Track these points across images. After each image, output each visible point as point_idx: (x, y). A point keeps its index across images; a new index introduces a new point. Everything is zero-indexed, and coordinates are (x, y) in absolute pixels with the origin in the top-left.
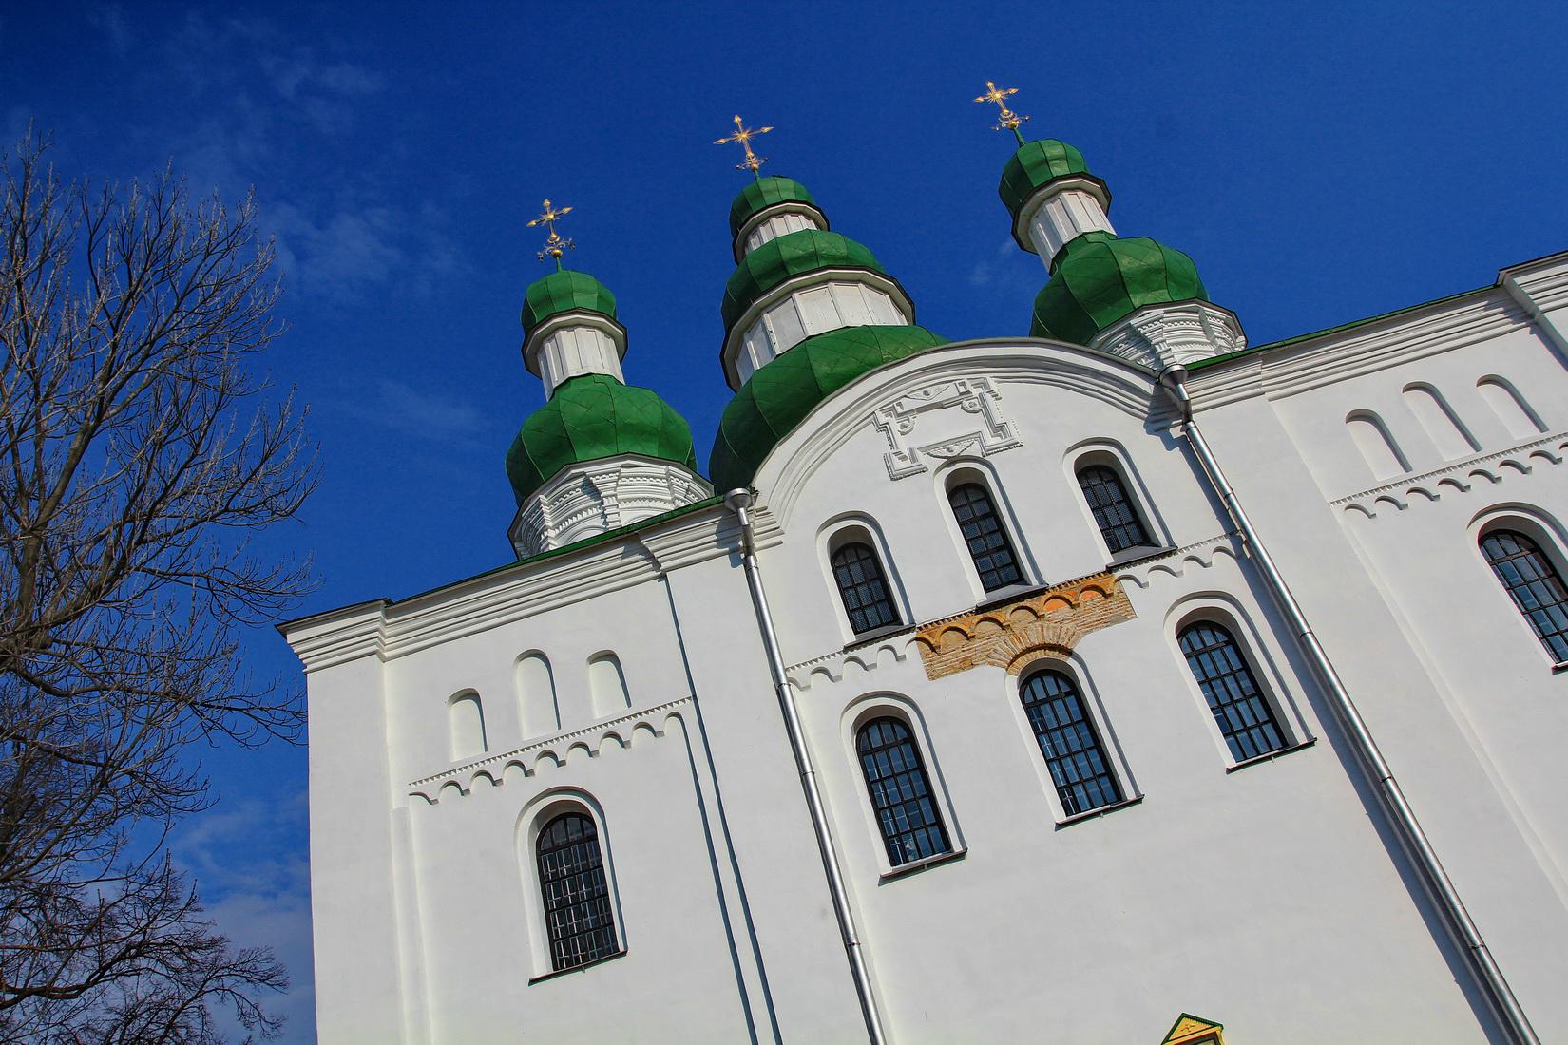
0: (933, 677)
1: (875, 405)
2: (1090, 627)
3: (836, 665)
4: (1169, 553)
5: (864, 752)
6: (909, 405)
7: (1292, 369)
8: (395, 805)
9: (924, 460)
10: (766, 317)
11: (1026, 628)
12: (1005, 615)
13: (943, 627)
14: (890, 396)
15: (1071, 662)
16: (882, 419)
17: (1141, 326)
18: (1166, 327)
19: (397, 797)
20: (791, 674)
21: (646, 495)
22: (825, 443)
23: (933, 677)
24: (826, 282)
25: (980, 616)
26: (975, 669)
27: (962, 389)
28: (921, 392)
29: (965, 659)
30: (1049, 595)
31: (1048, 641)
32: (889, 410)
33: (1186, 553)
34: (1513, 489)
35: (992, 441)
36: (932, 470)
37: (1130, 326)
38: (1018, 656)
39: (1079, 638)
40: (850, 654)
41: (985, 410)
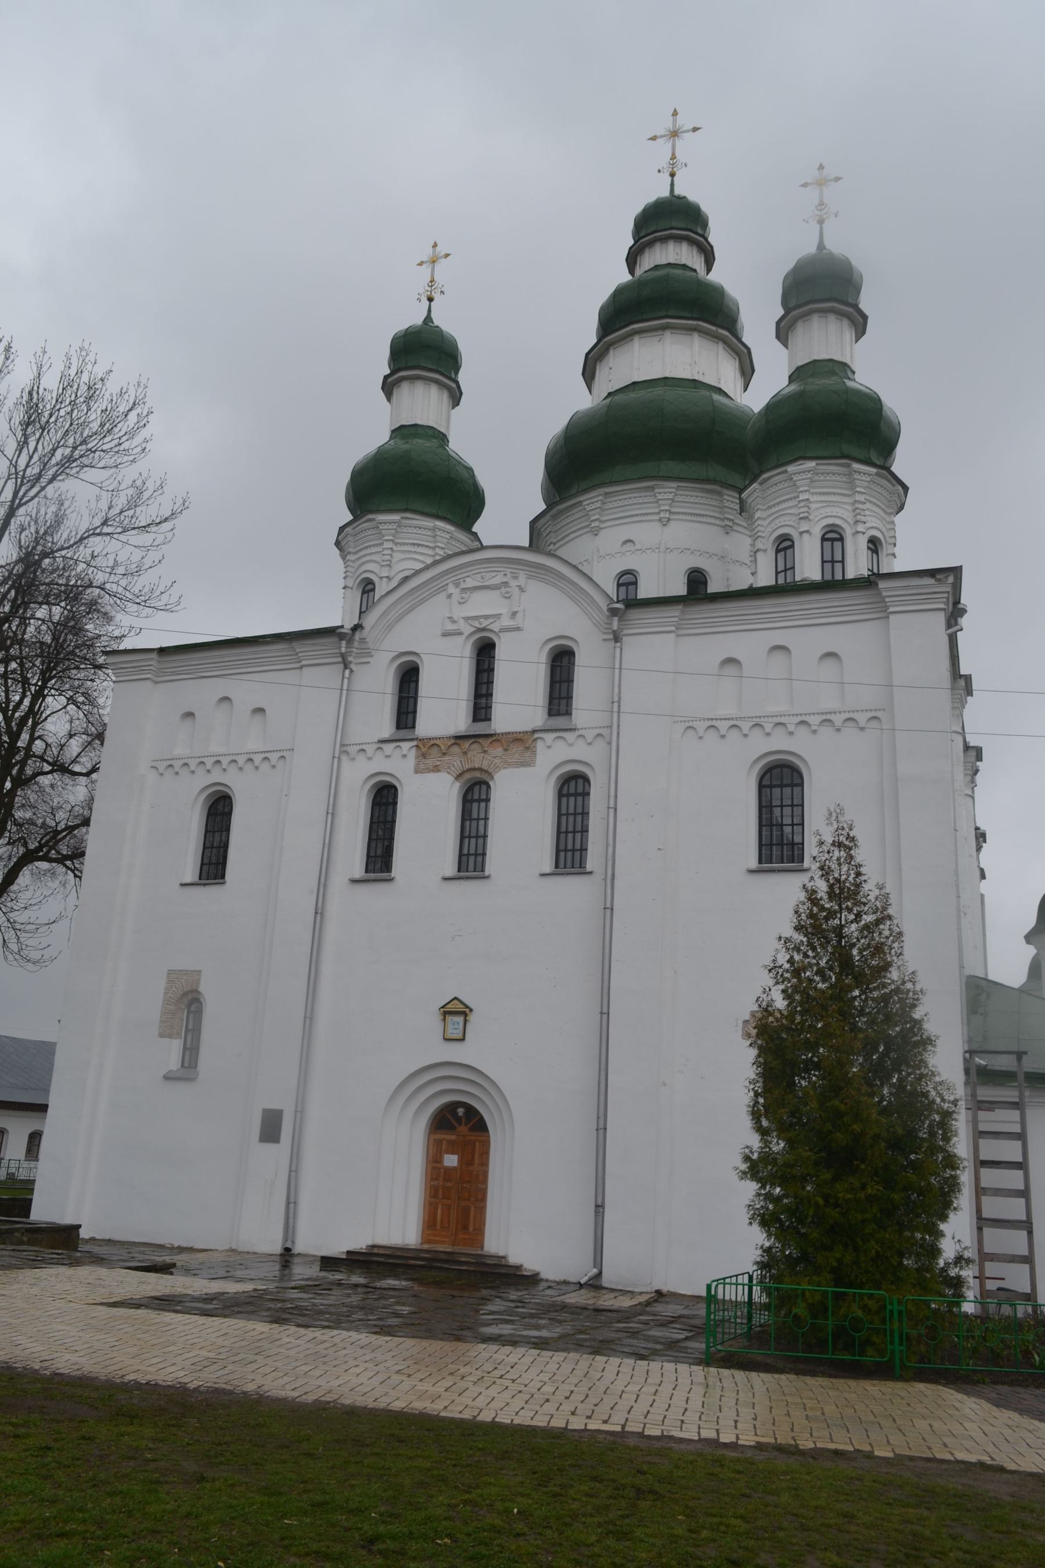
0: (417, 772)
2: (508, 765)
3: (370, 750)
4: (570, 730)
6: (470, 583)
7: (702, 616)
11: (474, 756)
12: (466, 744)
13: (432, 742)
15: (491, 783)
17: (795, 474)
18: (816, 478)
20: (348, 749)
21: (415, 542)
22: (413, 600)
23: (417, 772)
25: (453, 741)
26: (439, 774)
27: (504, 580)
28: (479, 576)
29: (436, 766)
30: (494, 738)
31: (483, 767)
32: (457, 585)
33: (581, 732)
35: (506, 622)
36: (466, 634)
37: (786, 472)
38: (464, 772)
39: (499, 771)
40: (381, 745)
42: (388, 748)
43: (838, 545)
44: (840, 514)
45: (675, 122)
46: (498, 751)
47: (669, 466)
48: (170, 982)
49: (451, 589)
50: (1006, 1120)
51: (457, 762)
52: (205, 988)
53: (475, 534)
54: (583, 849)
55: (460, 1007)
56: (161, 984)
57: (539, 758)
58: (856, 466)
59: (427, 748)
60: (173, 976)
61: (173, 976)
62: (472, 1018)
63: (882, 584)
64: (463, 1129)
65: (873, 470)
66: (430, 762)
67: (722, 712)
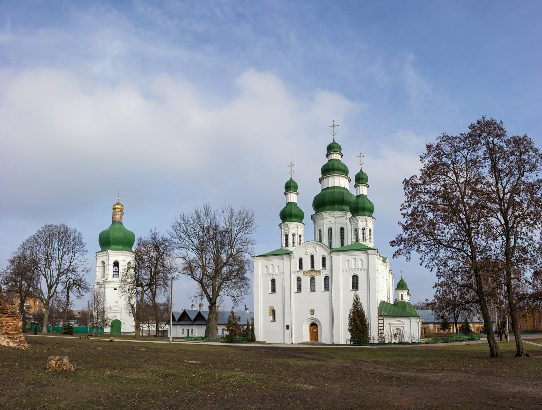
1: (306, 245)
2: (317, 275)
3: (296, 273)
5: (297, 280)
6: (309, 246)
8: (260, 276)
9: (308, 253)
10: (324, 179)
12: (311, 272)
14: (307, 245)
16: (306, 247)
19: (260, 275)
24: (334, 176)
34: (357, 273)
35: (315, 253)
41: (315, 249)
42: (299, 272)
43: (364, 230)
44: (364, 225)
45: (334, 123)
46: (315, 273)
47: (336, 206)
48: (269, 308)
49: (306, 247)
50: (381, 321)
51: (309, 274)
52: (275, 309)
53: (303, 223)
54: (328, 287)
55: (313, 310)
56: (268, 308)
57: (321, 274)
58: (367, 217)
59: (304, 272)
60: (270, 307)
61: (270, 307)
62: (315, 311)
63: (368, 250)
64: (314, 326)
65: (369, 217)
66: (305, 274)
67: (346, 268)
